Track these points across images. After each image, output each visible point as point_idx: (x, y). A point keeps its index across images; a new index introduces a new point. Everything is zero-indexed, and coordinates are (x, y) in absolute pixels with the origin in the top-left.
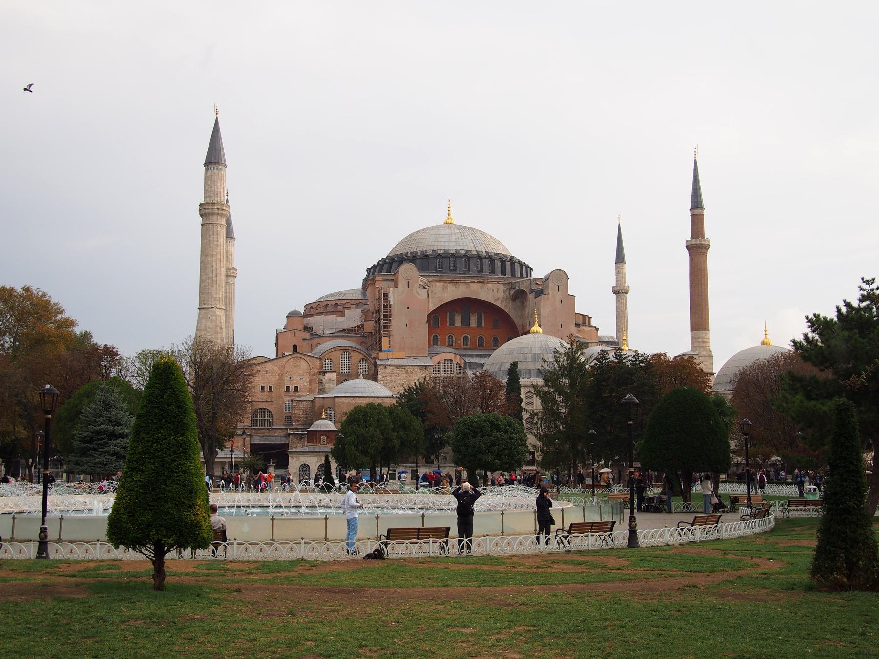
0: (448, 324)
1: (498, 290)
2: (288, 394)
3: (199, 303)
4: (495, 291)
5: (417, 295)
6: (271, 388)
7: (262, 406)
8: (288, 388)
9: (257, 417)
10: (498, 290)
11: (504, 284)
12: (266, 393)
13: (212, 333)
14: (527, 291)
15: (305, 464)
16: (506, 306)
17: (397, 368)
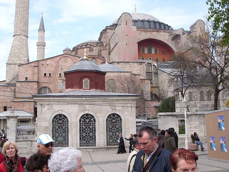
0: (142, 52)
1: (165, 35)
2: (60, 78)
3: (14, 33)
4: (164, 36)
5: (132, 29)
6: (50, 74)
7: (45, 85)
8: (60, 74)
9: (42, 92)
10: (165, 35)
11: (168, 32)
12: (47, 78)
13: (19, 48)
14: (181, 34)
15: (60, 115)
16: (169, 43)
17: (125, 64)
